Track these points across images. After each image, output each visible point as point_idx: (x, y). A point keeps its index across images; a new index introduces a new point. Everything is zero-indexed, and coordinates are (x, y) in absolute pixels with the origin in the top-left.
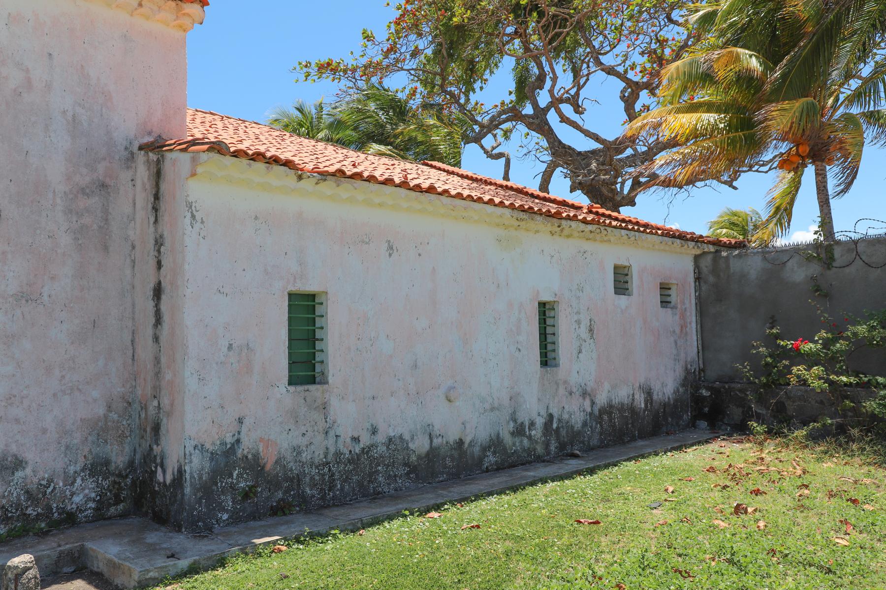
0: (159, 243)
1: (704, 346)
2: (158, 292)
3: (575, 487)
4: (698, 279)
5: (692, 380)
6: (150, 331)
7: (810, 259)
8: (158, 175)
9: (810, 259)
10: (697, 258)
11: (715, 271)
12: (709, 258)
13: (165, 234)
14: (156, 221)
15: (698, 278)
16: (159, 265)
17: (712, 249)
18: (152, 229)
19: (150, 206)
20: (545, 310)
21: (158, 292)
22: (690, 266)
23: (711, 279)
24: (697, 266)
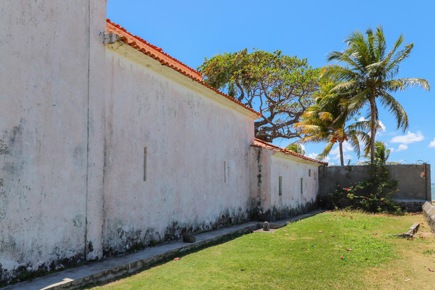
0: (260, 167)
1: (320, 189)
2: (259, 176)
3: (306, 221)
4: (319, 172)
5: (318, 197)
6: (256, 184)
7: (346, 169)
9: (346, 169)
10: (319, 167)
11: (323, 170)
12: (322, 167)
13: (262, 165)
14: (259, 162)
16: (260, 171)
17: (323, 165)
18: (257, 163)
19: (256, 159)
20: (302, 179)
21: (259, 176)
23: (323, 172)
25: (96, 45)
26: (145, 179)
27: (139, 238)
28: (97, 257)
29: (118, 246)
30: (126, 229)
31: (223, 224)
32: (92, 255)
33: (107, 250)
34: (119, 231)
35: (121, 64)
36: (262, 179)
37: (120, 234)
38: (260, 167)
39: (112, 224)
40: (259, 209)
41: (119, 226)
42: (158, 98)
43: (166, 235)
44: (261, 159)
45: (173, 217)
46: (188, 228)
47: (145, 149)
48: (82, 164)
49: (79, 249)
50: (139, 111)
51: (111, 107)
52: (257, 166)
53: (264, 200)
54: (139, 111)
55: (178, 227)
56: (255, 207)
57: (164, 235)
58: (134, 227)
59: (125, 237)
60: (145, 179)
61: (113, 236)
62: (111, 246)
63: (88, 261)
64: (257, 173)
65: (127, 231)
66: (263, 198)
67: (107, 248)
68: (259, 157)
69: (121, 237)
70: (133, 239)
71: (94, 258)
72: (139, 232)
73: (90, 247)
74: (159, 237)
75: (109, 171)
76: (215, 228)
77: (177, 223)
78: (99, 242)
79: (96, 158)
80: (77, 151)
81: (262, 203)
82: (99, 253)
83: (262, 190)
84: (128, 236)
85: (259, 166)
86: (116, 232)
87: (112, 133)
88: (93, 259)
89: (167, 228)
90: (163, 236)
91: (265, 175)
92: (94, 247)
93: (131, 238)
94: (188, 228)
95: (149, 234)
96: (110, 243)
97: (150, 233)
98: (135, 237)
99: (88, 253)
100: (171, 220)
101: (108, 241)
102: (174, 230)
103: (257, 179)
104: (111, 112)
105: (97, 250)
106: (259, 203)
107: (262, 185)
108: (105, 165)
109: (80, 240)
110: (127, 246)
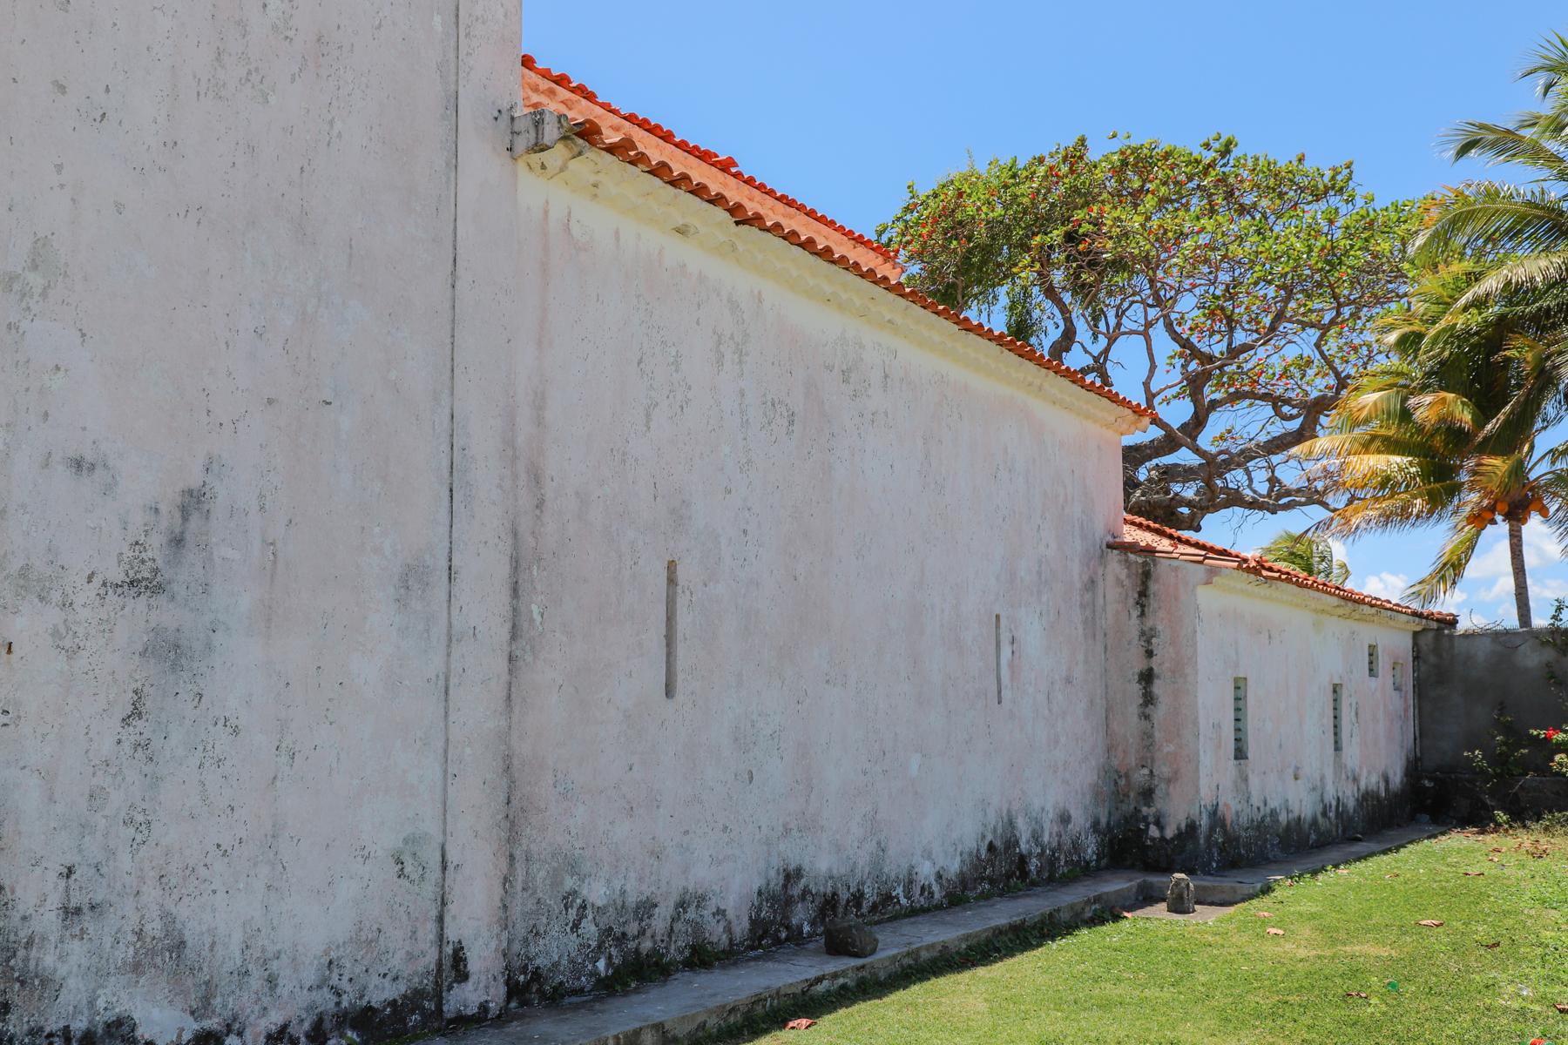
0: (1147, 636)
1: (1422, 733)
2: (1147, 677)
3: (1361, 874)
4: (1416, 658)
5: (1414, 769)
6: (1133, 709)
8: (1147, 575)
10: (1416, 634)
11: (1437, 650)
12: (1430, 635)
13: (1160, 628)
14: (1142, 614)
15: (1416, 658)
17: (1435, 625)
18: (1135, 621)
19: (1131, 601)
21: (1147, 677)
22: (1408, 642)
23: (1432, 659)
24: (1415, 644)
25: (481, 158)
26: (669, 691)
27: (648, 933)
28: (484, 1007)
29: (564, 962)
30: (597, 893)
31: (992, 881)
32: (465, 997)
33: (522, 978)
34: (568, 899)
35: (576, 230)
36: (1158, 688)
37: (573, 913)
38: (1147, 636)
39: (542, 874)
40: (1145, 818)
41: (569, 883)
42: (720, 360)
43: (755, 923)
44: (1153, 603)
45: (782, 847)
46: (844, 896)
47: (671, 567)
48: (428, 631)
49: (416, 973)
50: (648, 415)
51: (539, 405)
52: (1135, 633)
53: (1169, 781)
54: (648, 415)
55: (806, 892)
56: (1128, 808)
57: (746, 924)
58: (628, 888)
59: (593, 928)
60: (669, 691)
61: (544, 920)
62: (538, 962)
63: (450, 1021)
64: (1139, 665)
65: (599, 903)
66: (1163, 770)
67: (524, 970)
68: (1143, 594)
69: (576, 926)
70: (624, 934)
71: (472, 1010)
72: (646, 908)
73: (456, 966)
74: (728, 929)
75: (529, 658)
76: (958, 895)
77: (798, 873)
78: (493, 944)
79: (482, 606)
80: (411, 579)
81: (1158, 793)
82: (492, 991)
83: (1157, 735)
84: (604, 921)
85: (1143, 633)
86: (556, 906)
87: (540, 505)
88: (469, 1012)
89: (760, 893)
90: (741, 927)
91: (1173, 672)
92: (474, 965)
93: (617, 930)
94: (844, 896)
95: (687, 916)
96: (533, 950)
97: (691, 914)
98: (633, 928)
99: (450, 988)
100: (776, 862)
101: (526, 940)
102: (789, 902)
103: (1136, 689)
104: (540, 422)
105: (483, 978)
106: (1148, 794)
107: (1160, 713)
108: (514, 634)
109: (420, 934)
110: (601, 965)
